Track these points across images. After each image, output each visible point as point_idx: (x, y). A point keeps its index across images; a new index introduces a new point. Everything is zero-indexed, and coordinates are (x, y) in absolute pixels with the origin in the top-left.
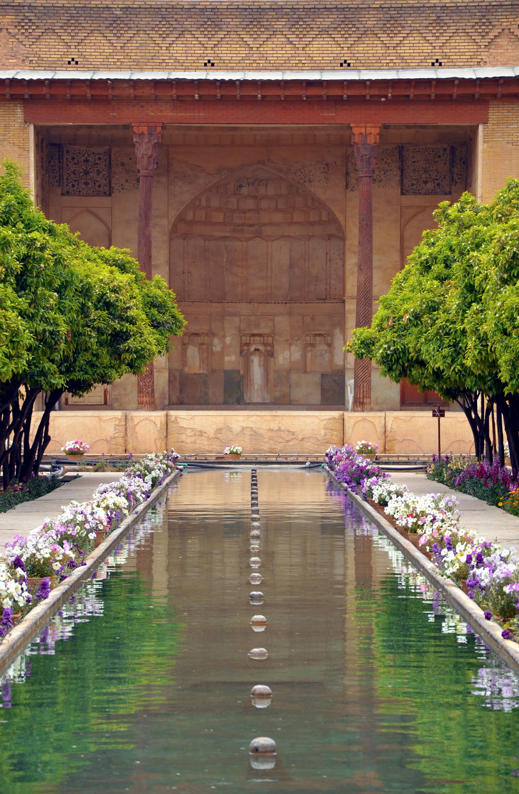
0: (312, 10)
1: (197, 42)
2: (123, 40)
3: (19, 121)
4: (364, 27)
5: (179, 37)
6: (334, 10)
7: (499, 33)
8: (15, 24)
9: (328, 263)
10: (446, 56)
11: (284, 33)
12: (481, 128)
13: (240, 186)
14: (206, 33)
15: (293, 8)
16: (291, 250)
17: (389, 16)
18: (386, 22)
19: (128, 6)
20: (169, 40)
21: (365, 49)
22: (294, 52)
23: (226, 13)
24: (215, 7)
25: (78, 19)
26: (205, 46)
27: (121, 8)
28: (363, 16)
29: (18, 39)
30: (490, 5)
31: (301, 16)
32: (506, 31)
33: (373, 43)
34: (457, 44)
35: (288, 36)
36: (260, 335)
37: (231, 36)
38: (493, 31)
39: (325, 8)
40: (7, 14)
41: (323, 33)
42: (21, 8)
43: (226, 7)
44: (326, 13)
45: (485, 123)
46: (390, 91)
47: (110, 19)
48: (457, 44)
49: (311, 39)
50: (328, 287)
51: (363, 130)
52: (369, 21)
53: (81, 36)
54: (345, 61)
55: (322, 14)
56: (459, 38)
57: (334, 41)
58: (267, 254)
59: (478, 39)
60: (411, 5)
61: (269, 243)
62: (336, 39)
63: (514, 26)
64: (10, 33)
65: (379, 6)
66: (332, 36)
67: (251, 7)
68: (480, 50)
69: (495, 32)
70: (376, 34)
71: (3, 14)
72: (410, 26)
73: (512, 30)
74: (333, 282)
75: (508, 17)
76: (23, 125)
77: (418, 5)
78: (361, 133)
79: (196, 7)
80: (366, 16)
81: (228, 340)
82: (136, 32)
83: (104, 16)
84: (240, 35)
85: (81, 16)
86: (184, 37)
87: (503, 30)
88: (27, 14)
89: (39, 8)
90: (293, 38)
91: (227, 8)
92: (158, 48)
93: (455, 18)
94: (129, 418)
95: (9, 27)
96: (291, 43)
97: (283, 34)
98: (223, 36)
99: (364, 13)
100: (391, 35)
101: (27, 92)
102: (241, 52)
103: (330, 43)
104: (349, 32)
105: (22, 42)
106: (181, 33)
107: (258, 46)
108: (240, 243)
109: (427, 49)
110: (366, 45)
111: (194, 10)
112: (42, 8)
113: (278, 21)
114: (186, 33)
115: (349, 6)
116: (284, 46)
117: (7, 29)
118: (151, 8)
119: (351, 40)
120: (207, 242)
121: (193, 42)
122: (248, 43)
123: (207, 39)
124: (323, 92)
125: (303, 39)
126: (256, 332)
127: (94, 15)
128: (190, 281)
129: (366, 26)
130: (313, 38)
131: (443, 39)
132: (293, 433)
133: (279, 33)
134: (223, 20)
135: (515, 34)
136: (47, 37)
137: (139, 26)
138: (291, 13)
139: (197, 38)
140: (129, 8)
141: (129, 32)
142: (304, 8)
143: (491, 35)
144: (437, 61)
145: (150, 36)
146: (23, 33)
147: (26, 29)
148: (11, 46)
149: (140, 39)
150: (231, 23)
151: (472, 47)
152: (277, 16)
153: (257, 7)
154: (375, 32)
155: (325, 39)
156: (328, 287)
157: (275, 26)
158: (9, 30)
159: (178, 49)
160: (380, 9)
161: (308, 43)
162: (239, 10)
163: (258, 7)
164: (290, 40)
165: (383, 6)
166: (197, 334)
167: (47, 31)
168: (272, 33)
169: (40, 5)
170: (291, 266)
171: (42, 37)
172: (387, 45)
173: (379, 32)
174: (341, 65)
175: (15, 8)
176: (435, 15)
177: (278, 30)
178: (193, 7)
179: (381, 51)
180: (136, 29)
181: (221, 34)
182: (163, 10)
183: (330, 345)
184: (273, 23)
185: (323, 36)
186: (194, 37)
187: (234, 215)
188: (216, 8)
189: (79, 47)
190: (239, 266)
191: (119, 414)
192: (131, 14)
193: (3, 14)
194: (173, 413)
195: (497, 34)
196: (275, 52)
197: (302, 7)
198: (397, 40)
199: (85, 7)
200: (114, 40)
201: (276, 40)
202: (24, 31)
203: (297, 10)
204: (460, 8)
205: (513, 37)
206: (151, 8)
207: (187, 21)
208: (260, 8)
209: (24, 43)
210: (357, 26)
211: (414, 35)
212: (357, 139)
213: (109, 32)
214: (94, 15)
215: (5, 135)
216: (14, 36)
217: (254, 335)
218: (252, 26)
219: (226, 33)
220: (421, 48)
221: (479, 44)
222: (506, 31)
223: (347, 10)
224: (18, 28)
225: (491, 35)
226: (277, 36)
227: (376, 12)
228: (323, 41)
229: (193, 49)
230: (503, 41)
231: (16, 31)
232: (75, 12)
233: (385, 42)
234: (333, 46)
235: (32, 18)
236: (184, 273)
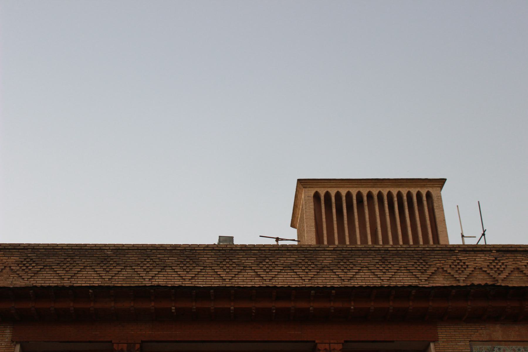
0: (276, 252)
1: (176, 276)
2: (112, 273)
3: (6, 340)
4: (321, 264)
5: (161, 272)
6: (295, 252)
7: (435, 270)
8: (17, 263)
11: (253, 268)
12: (432, 345)
14: (185, 268)
15: (260, 250)
17: (342, 256)
18: (340, 261)
19: (118, 248)
20: (152, 273)
21: (323, 281)
22: (262, 283)
23: (202, 254)
24: (193, 248)
25: (73, 257)
26: (184, 278)
27: (112, 249)
28: (320, 256)
29: (18, 274)
30: (424, 250)
31: (267, 256)
33: (330, 277)
34: (401, 279)
35: (256, 271)
37: (207, 271)
38: (429, 269)
39: (288, 250)
40: (12, 255)
41: (287, 268)
42: (25, 251)
43: (202, 248)
44: (289, 254)
45: (435, 341)
46: (353, 304)
47: (102, 258)
48: (401, 279)
49: (277, 273)
51: (327, 346)
52: (325, 260)
53: (75, 270)
55: (285, 255)
56: (402, 274)
57: (297, 275)
59: (419, 274)
60: (360, 249)
62: (298, 273)
63: (447, 266)
64: (12, 269)
65: (332, 249)
66: (295, 271)
67: (224, 249)
68: (422, 283)
69: (432, 270)
70: (332, 270)
71: (9, 255)
72: (360, 265)
73: (445, 269)
75: (440, 259)
76: (9, 344)
77: (365, 249)
78: (326, 349)
79: (177, 248)
80: (323, 256)
82: (123, 267)
83: (97, 255)
84: (214, 269)
85: (77, 256)
86: (166, 272)
87: (438, 268)
88: (29, 255)
89: (41, 250)
91: (204, 250)
92: (142, 280)
93: (397, 259)
95: (11, 265)
96: (259, 276)
97: (252, 270)
98: (200, 270)
99: (321, 254)
100: (345, 271)
102: (215, 283)
103: (293, 276)
104: (309, 268)
105: (21, 276)
106: (163, 268)
107: (231, 278)
110: (324, 279)
111: (175, 251)
112: (43, 250)
113: (247, 260)
114: (167, 268)
115: (308, 249)
116: (253, 278)
117: (10, 267)
118: (138, 249)
119: (311, 274)
121: (173, 276)
122: (222, 275)
123: (186, 273)
125: (270, 273)
127: (88, 256)
129: (323, 264)
130: (278, 272)
131: (389, 275)
133: (249, 269)
134: (200, 259)
135: (448, 272)
136: (44, 272)
137: (127, 263)
138: (259, 254)
139: (177, 272)
140: (119, 249)
141: (117, 267)
142: (269, 250)
143: (429, 272)
145: (136, 270)
146: (24, 270)
147: (27, 267)
148: (11, 280)
149: (126, 273)
150: (207, 261)
151: (414, 281)
152: (246, 256)
153: (229, 249)
154: (331, 268)
155: (288, 274)
157: (245, 263)
158: (12, 268)
160: (334, 252)
161: (274, 276)
162: (214, 251)
163: (231, 249)
164: (258, 273)
165: (336, 249)
167: (45, 268)
168: (242, 268)
169: (42, 247)
171: (40, 272)
172: (343, 278)
173: (335, 268)
175: (20, 251)
176: (380, 256)
177: (248, 266)
178: (175, 248)
180: (124, 265)
181: (198, 269)
182: (148, 251)
184: (244, 261)
185: (286, 271)
186: (175, 272)
188: (194, 250)
189: (71, 280)
192: (120, 254)
193: (9, 255)
195: (433, 271)
196: (246, 283)
197: (268, 249)
198: (350, 274)
199: (81, 249)
200: (103, 274)
201: (246, 274)
202: (25, 268)
203: (263, 251)
204: (400, 252)
205: (446, 274)
206: (138, 249)
207: (168, 259)
208: (232, 250)
209: (23, 277)
210: (315, 263)
211: (364, 271)
213: (99, 267)
214: (88, 256)
216: (16, 272)
218: (225, 263)
219: (202, 268)
220: (371, 281)
221: (420, 278)
222: (441, 270)
223: (307, 251)
224: (20, 265)
225: (429, 272)
226: (247, 271)
227: (330, 254)
228: (287, 275)
229: (172, 280)
231: (18, 268)
232: (72, 252)
233: (340, 276)
234: (296, 279)
235: (34, 257)
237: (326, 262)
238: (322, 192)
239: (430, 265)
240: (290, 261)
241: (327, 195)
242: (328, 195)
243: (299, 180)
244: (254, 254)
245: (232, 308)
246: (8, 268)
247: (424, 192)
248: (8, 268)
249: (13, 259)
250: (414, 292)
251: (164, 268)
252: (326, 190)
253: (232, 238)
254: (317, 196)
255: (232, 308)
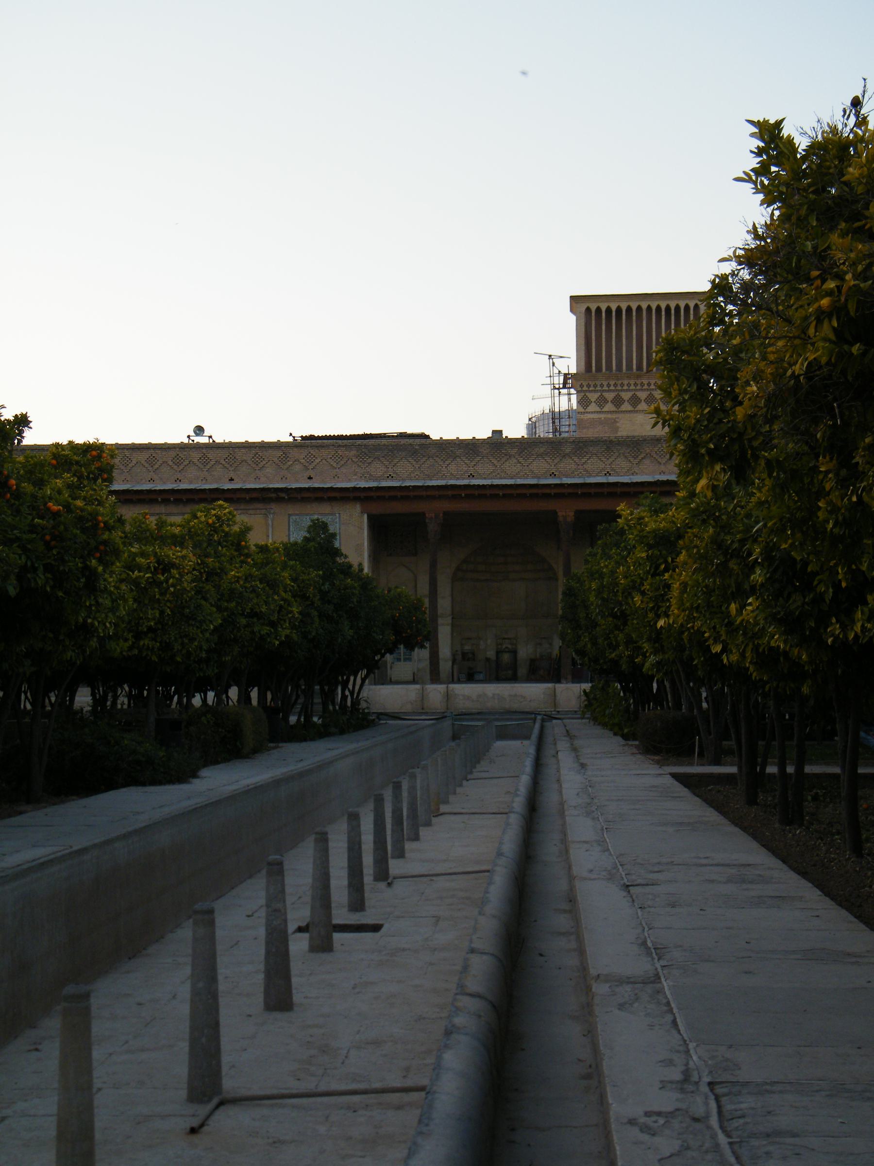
10: (613, 470)
20: (447, 462)
32: (649, 455)
36: (508, 639)
51: (564, 514)
54: (553, 473)
59: (632, 460)
64: (353, 461)
69: (642, 456)
81: (489, 641)
87: (647, 454)
90: (521, 460)
94: (424, 689)
96: (520, 463)
101: (363, 495)
109: (602, 465)
124: (540, 491)
126: (506, 637)
131: (611, 460)
132: (524, 697)
143: (640, 457)
144: (608, 472)
159: (453, 468)
166: (469, 639)
174: (551, 475)
179: (573, 466)
181: (478, 458)
183: (551, 644)
191: (418, 686)
194: (451, 686)
198: (583, 460)
212: (561, 519)
215: (350, 520)
217: (504, 639)
222: (649, 455)
225: (640, 457)
230: (647, 461)
237: (568, 451)
238: (593, 308)
239: (641, 452)
240: (542, 450)
241: (598, 310)
242: (598, 310)
243: (571, 297)
244: (517, 446)
245: (501, 494)
246: (350, 460)
247: (692, 305)
248: (350, 460)
249: (353, 452)
250: (619, 484)
251: (455, 458)
252: (597, 306)
253: (501, 432)
254: (588, 310)
255: (501, 494)
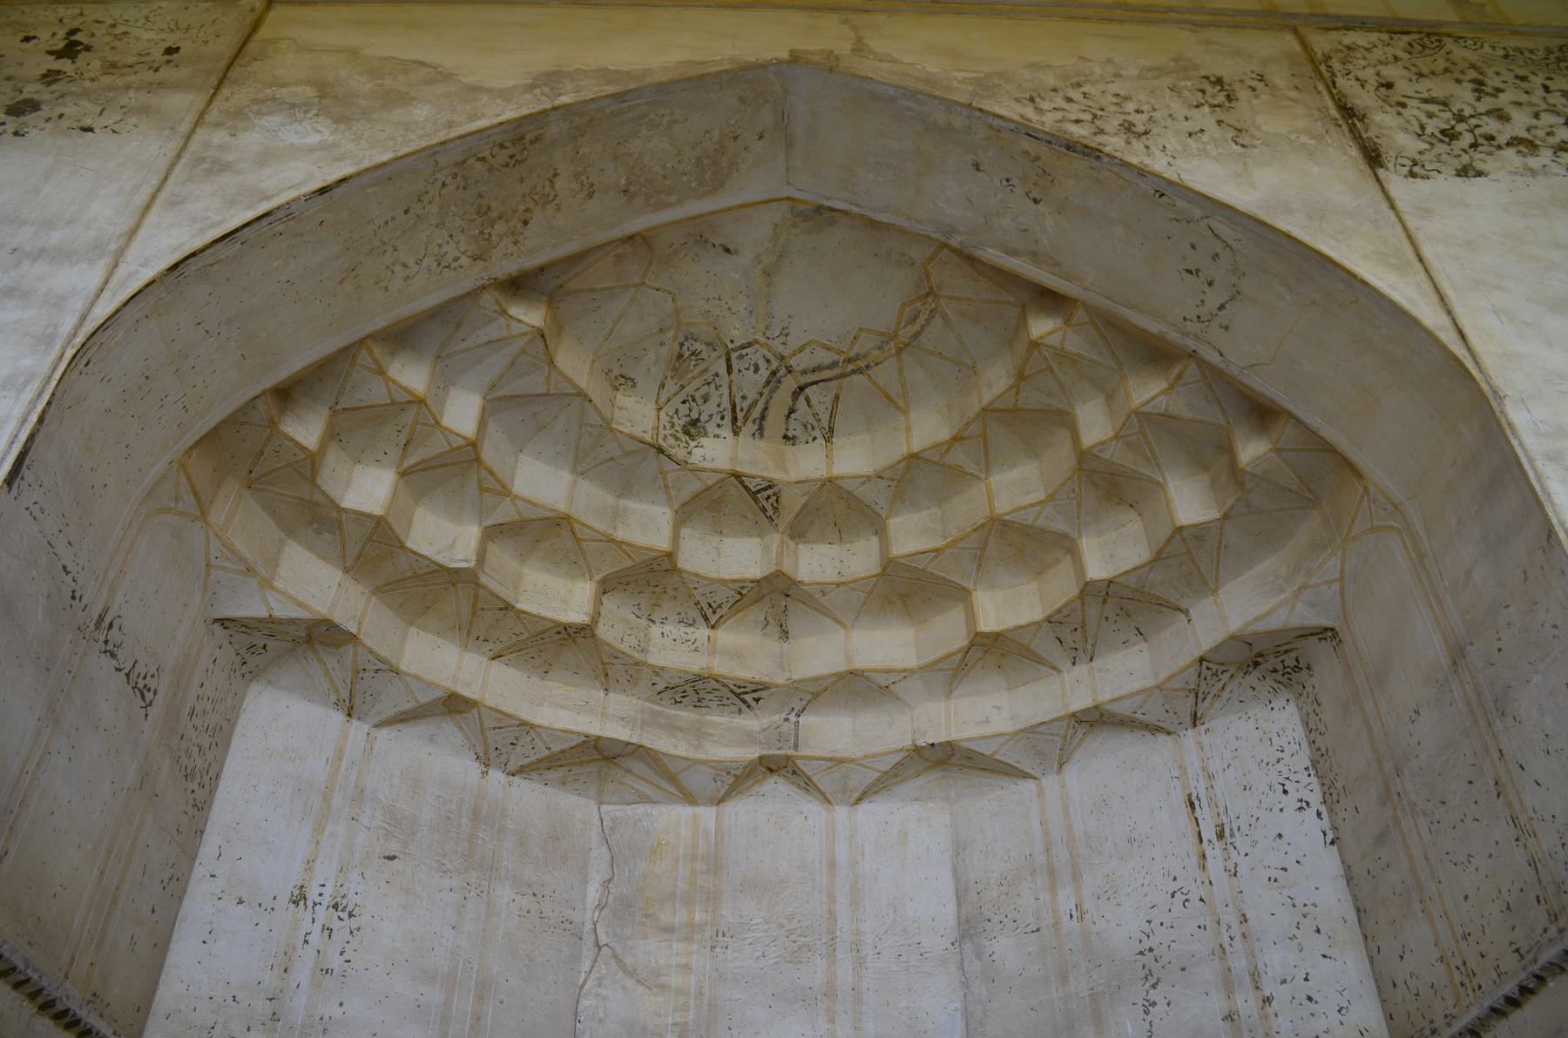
9: (1214, 852)
13: (693, 428)
16: (959, 848)
50: (1246, 1003)
58: (832, 865)
61: (841, 812)
74: (1276, 960)
108: (686, 811)
120: (496, 776)
128: (335, 962)
156: (1246, 1003)
170: (969, 929)
187: (656, 630)
190: (669, 929)
236: (299, 898)
